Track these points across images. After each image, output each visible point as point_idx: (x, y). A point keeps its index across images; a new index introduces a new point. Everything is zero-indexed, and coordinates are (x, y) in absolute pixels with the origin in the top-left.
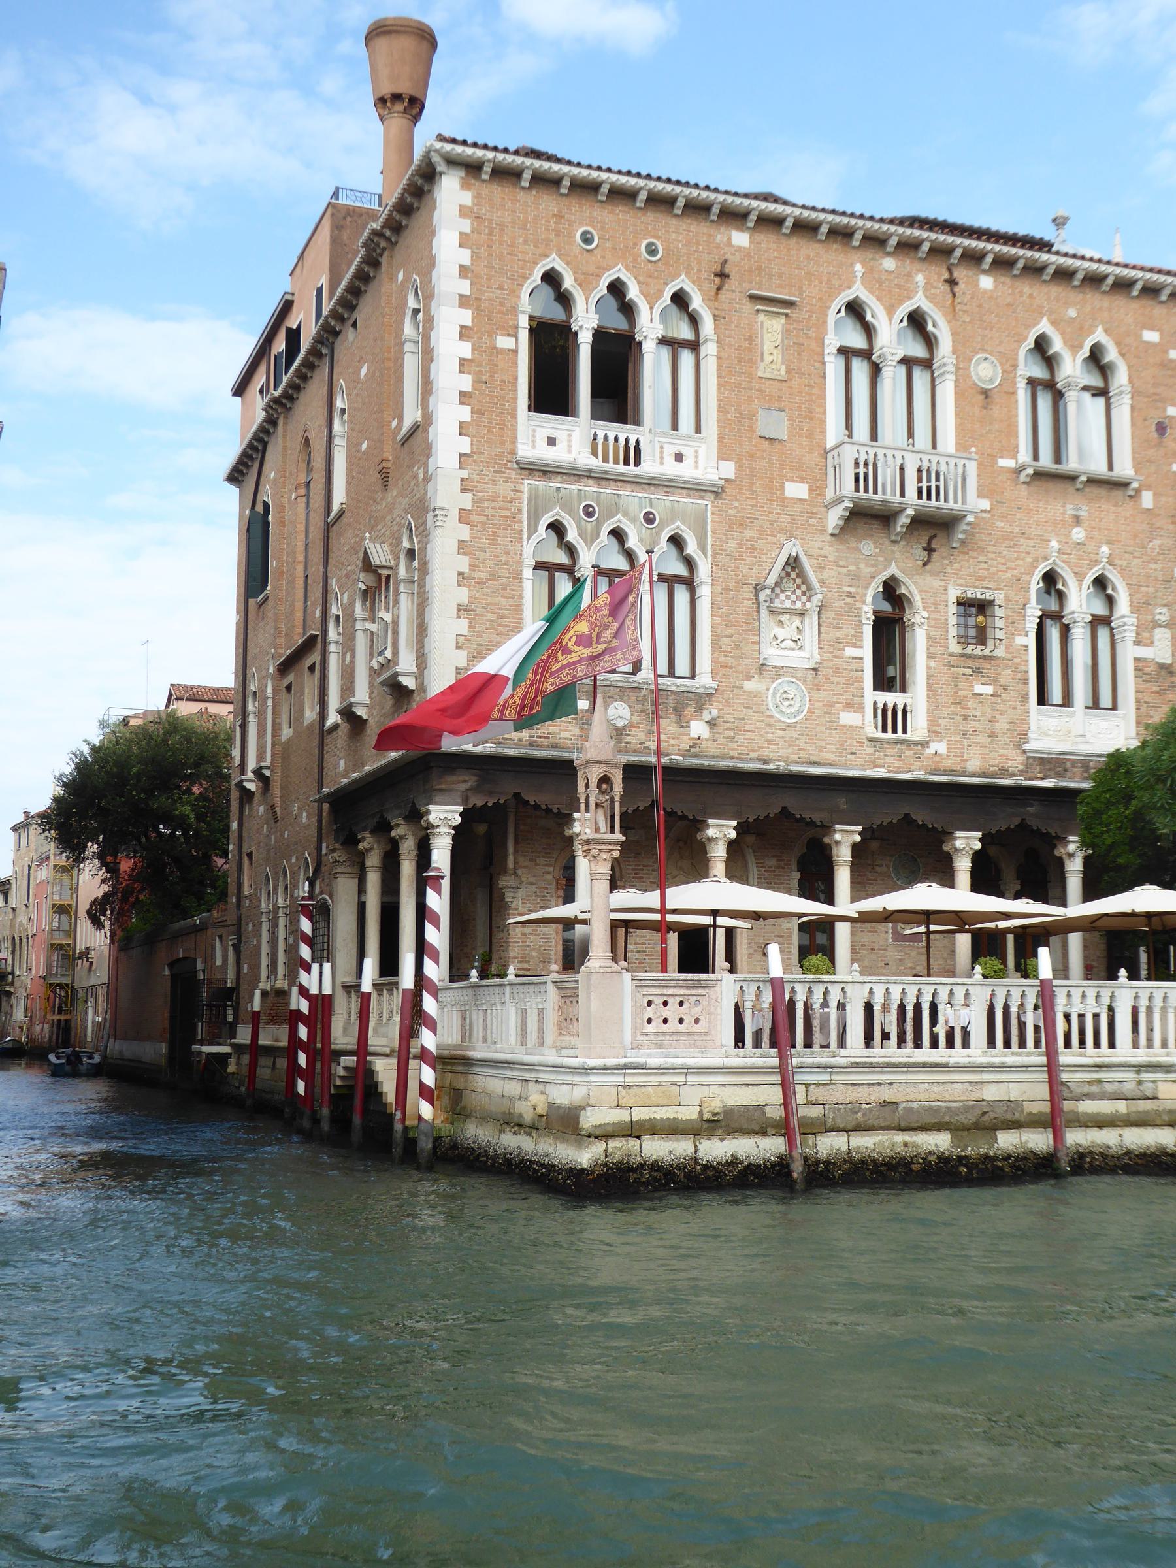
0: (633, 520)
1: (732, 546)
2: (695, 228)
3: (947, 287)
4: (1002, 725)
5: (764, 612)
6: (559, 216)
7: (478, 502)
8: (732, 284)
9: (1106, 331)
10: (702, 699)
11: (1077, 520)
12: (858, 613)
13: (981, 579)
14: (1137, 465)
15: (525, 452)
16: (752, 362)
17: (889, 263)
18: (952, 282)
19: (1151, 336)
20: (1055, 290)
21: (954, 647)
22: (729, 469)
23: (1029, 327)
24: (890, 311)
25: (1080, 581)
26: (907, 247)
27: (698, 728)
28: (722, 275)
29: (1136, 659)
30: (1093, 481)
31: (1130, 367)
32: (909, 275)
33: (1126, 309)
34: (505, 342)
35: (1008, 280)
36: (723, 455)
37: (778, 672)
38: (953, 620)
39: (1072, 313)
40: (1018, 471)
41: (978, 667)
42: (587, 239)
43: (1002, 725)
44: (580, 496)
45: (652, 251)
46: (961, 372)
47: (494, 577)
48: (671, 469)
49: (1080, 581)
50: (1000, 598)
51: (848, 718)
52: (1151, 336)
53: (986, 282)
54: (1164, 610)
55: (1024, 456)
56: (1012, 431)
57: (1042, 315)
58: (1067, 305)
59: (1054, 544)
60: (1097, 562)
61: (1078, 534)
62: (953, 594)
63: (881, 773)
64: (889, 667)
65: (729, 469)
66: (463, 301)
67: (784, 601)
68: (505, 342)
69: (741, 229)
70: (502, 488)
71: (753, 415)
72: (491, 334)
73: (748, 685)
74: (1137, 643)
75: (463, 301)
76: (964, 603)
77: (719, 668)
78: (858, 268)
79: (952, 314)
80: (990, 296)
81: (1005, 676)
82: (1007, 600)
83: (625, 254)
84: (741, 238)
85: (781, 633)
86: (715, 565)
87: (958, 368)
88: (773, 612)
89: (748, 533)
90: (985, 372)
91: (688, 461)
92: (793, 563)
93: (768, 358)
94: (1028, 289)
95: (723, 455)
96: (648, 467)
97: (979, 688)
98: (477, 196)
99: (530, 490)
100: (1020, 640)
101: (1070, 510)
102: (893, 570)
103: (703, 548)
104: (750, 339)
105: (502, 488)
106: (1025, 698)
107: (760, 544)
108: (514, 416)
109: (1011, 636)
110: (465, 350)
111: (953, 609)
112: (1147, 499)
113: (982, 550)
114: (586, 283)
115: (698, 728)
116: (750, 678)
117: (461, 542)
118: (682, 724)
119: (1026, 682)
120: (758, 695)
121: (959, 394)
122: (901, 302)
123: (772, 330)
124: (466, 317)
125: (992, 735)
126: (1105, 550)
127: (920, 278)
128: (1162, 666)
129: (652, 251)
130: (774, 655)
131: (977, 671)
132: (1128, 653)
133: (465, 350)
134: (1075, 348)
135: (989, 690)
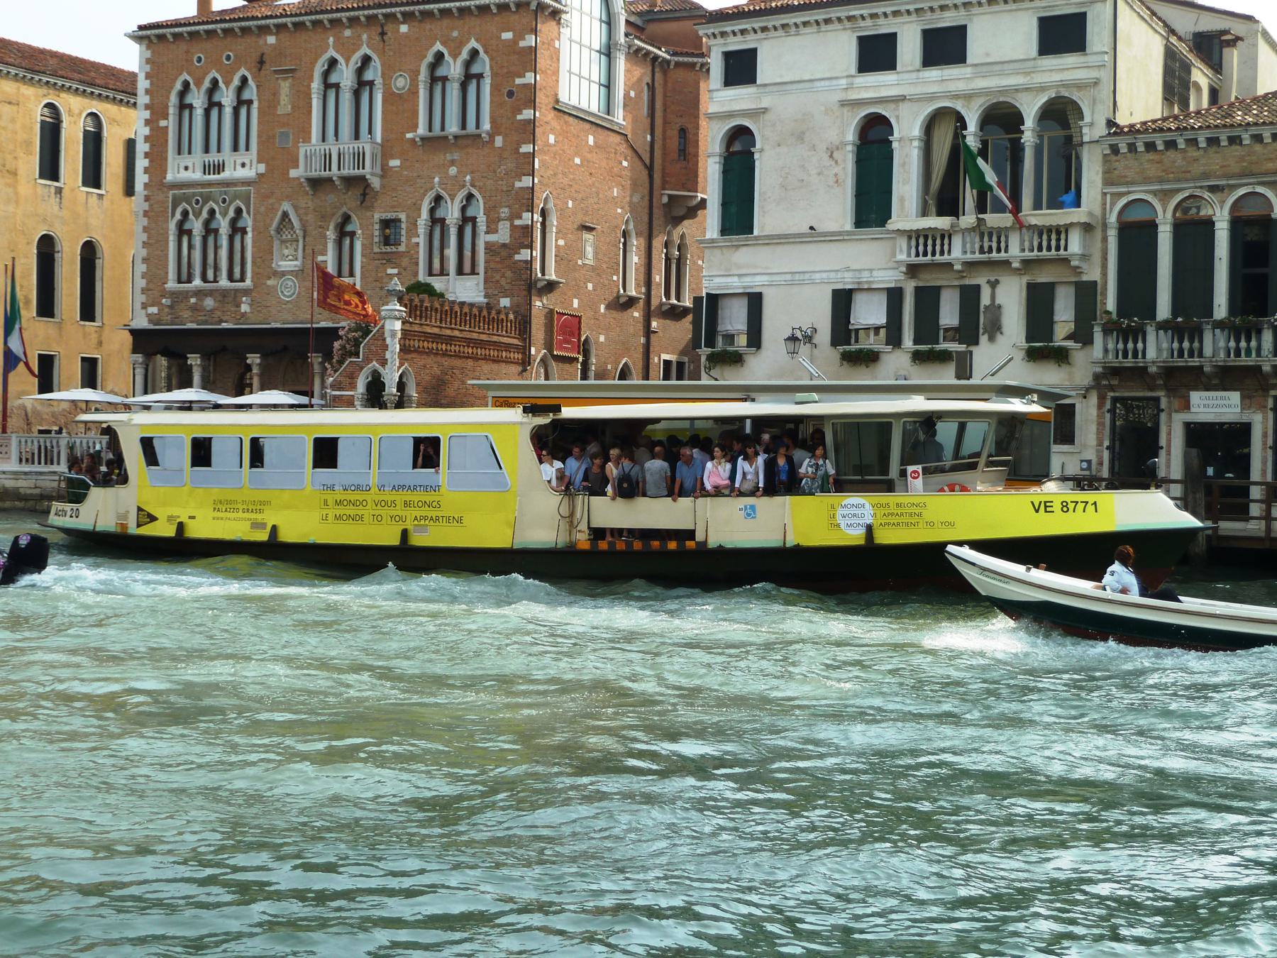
0: (217, 203)
1: (263, 209)
2: (249, 40)
3: (378, 38)
5: (276, 244)
6: (187, 52)
7: (151, 206)
8: (266, 66)
9: (477, 40)
10: (246, 292)
11: (453, 163)
12: (325, 237)
13: (393, 207)
14: (493, 122)
16: (275, 107)
17: (348, 33)
18: (383, 34)
19: (508, 36)
20: (446, 22)
22: (262, 168)
23: (427, 50)
24: (347, 60)
25: (452, 200)
26: (353, 21)
28: (261, 62)
29: (486, 243)
31: (491, 59)
32: (360, 36)
33: (490, 25)
34: (163, 123)
35: (416, 24)
36: (259, 161)
37: (283, 274)
38: (377, 233)
39: (455, 34)
40: (413, 140)
41: (390, 259)
42: (199, 60)
44: (194, 194)
45: (228, 58)
46: (387, 87)
47: (158, 241)
48: (242, 173)
49: (452, 200)
50: (403, 217)
52: (508, 36)
53: (404, 28)
54: (506, 210)
55: (422, 130)
57: (436, 39)
58: (452, 29)
59: (437, 179)
60: (464, 186)
61: (453, 171)
62: (377, 216)
65: (262, 168)
67: (286, 235)
68: (163, 123)
69: (271, 34)
70: (161, 197)
71: (274, 136)
72: (157, 121)
73: (269, 282)
74: (487, 233)
75: (147, 107)
77: (255, 274)
78: (331, 39)
79: (382, 54)
80: (406, 36)
82: (408, 217)
83: (217, 64)
84: (271, 40)
85: (286, 252)
86: (254, 220)
87: (384, 85)
88: (283, 242)
89: (271, 201)
90: (401, 83)
91: (248, 167)
92: (285, 215)
93: (282, 103)
95: (259, 161)
97: (390, 271)
98: (153, 53)
99: (174, 195)
100: (414, 240)
101: (449, 157)
102: (344, 209)
103: (248, 213)
104: (274, 94)
105: (161, 197)
107: (276, 206)
108: (166, 159)
109: (409, 239)
111: (377, 226)
112: (499, 141)
113: (395, 190)
114: (199, 84)
115: (245, 308)
116: (269, 278)
117: (144, 228)
118: (238, 306)
119: (417, 264)
120: (275, 287)
121: (385, 101)
122: (354, 52)
123: (285, 87)
124: (147, 114)
126: (468, 178)
127: (365, 37)
128: (504, 245)
129: (228, 58)
131: (389, 261)
132: (483, 239)
135: (395, 271)
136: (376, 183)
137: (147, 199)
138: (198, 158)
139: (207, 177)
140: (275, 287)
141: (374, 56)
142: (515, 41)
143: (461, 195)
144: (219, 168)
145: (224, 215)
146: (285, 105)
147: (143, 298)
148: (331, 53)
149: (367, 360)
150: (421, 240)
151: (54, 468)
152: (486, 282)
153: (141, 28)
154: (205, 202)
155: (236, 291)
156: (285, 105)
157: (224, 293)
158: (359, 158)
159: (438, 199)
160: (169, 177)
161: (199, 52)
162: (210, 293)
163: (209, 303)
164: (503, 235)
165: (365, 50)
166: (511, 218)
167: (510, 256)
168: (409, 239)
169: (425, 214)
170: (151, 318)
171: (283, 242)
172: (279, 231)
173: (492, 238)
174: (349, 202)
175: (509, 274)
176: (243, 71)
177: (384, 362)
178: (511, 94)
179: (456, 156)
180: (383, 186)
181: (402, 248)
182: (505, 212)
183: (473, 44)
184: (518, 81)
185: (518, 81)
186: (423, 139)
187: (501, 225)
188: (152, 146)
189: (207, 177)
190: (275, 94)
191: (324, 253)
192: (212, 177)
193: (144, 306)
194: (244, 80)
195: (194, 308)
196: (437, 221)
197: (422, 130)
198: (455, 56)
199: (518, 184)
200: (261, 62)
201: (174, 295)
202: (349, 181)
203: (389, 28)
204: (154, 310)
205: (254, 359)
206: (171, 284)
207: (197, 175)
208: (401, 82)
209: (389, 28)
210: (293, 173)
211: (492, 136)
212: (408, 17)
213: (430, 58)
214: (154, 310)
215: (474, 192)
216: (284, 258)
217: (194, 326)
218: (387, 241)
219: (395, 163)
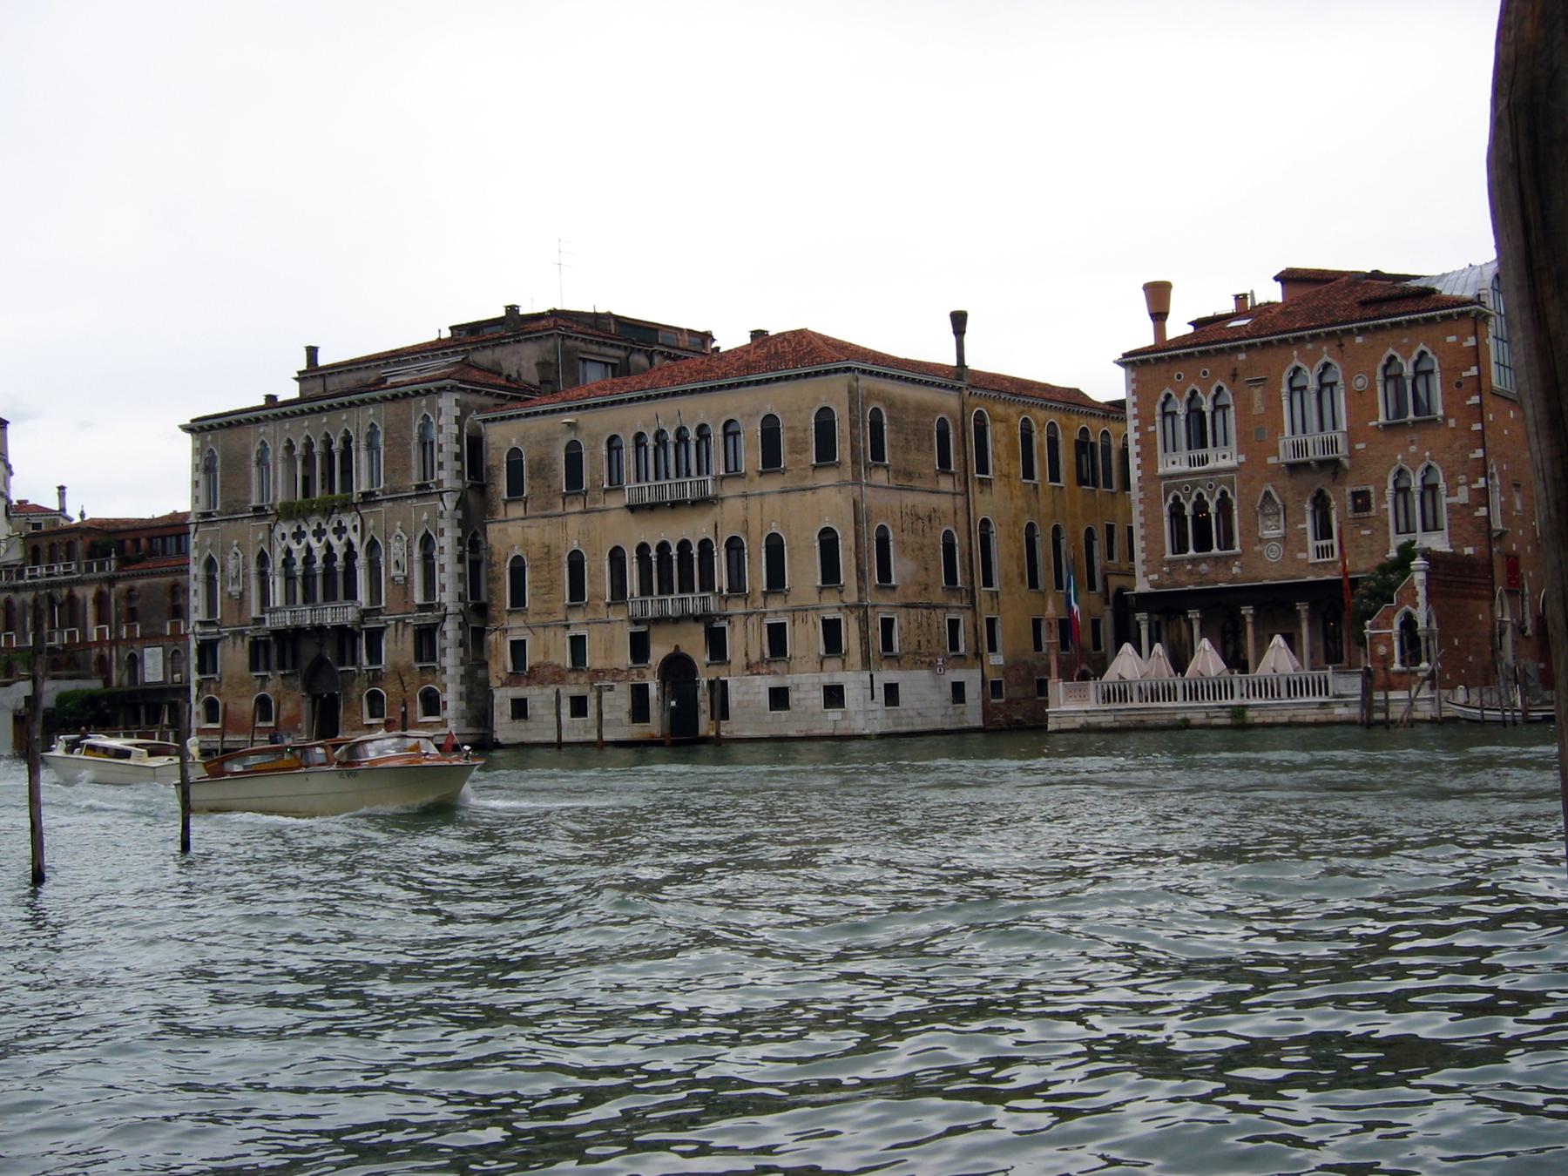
4: (1376, 547)
10: (1236, 557)
11: (1412, 442)
14: (1445, 407)
15: (1160, 471)
17: (1309, 346)
18: (1341, 345)
20: (1395, 332)
21: (1350, 516)
22: (1242, 458)
25: (1415, 471)
26: (1314, 337)
27: (1235, 570)
28: (1234, 375)
30: (1414, 422)
31: (1439, 359)
34: (1151, 429)
36: (1239, 453)
41: (1363, 523)
43: (1376, 547)
48: (1223, 464)
50: (1371, 489)
51: (1301, 556)
53: (1359, 340)
55: (1382, 419)
56: (1376, 405)
61: (1413, 449)
62: (1348, 491)
63: (1310, 578)
64: (1324, 531)
65: (1242, 458)
66: (1135, 417)
67: (1268, 510)
68: (1151, 429)
73: (1257, 548)
75: (1135, 417)
76: (1355, 495)
81: (1376, 524)
84: (1242, 356)
90: (1360, 383)
92: (1268, 494)
94: (1380, 336)
95: (1239, 453)
96: (1211, 465)
101: (1408, 438)
102: (1319, 486)
106: (1387, 533)
110: (1137, 436)
112: (1452, 423)
114: (1180, 395)
115: (1235, 570)
120: (1261, 553)
121: (1347, 397)
125: (1371, 553)
130: (1268, 534)
132: (1444, 501)
133: (1137, 436)
134: (1407, 358)
136: (1346, 463)
137: (1141, 489)
138: (1184, 454)
139: (1194, 469)
140: (1261, 553)
141: (1335, 363)
142: (1459, 342)
143: (1422, 467)
144: (1204, 461)
145: (1212, 497)
146: (1258, 406)
147: (1144, 568)
148: (1296, 363)
149: (1400, 604)
150: (1390, 506)
151: (1129, 705)
152: (1450, 535)
153: (1125, 355)
154: (1194, 487)
155: (1228, 557)
156: (1258, 406)
157: (1217, 558)
158: (1332, 445)
159: (1401, 472)
160: (1160, 471)
161: (1177, 371)
162: (1204, 560)
163: (1204, 567)
164: (1463, 496)
165: (1326, 358)
166: (1468, 484)
167: (1470, 514)
168: (1378, 505)
169: (1390, 486)
170: (1152, 583)
171: (1266, 515)
172: (1262, 507)
173: (1451, 500)
174: (1322, 481)
175: (1471, 528)
176: (1219, 383)
177: (1415, 605)
178: (1459, 385)
179: (1415, 437)
180: (1352, 466)
181: (1373, 513)
182: (1462, 478)
183: (1422, 347)
184: (1465, 374)
185: (1465, 374)
186: (1385, 426)
187: (1460, 489)
188: (1143, 447)
189: (1194, 469)
190: (1249, 400)
191: (1303, 521)
192: (1197, 468)
193: (1145, 575)
194: (1220, 389)
195: (1190, 573)
196: (1402, 491)
197: (1382, 419)
198: (1407, 358)
199: (1472, 456)
200: (1234, 375)
201: (1169, 562)
202: (1322, 464)
203: (1345, 341)
204: (1155, 577)
205: (1247, 611)
206: (1169, 555)
207: (1185, 468)
208: (1360, 382)
209: (1345, 341)
210: (1271, 460)
211: (1445, 418)
212: (1362, 331)
213: (1384, 361)
214: (1155, 577)
215: (1434, 464)
216: (1268, 528)
217: (1191, 587)
218: (1356, 509)
219: (1360, 446)
